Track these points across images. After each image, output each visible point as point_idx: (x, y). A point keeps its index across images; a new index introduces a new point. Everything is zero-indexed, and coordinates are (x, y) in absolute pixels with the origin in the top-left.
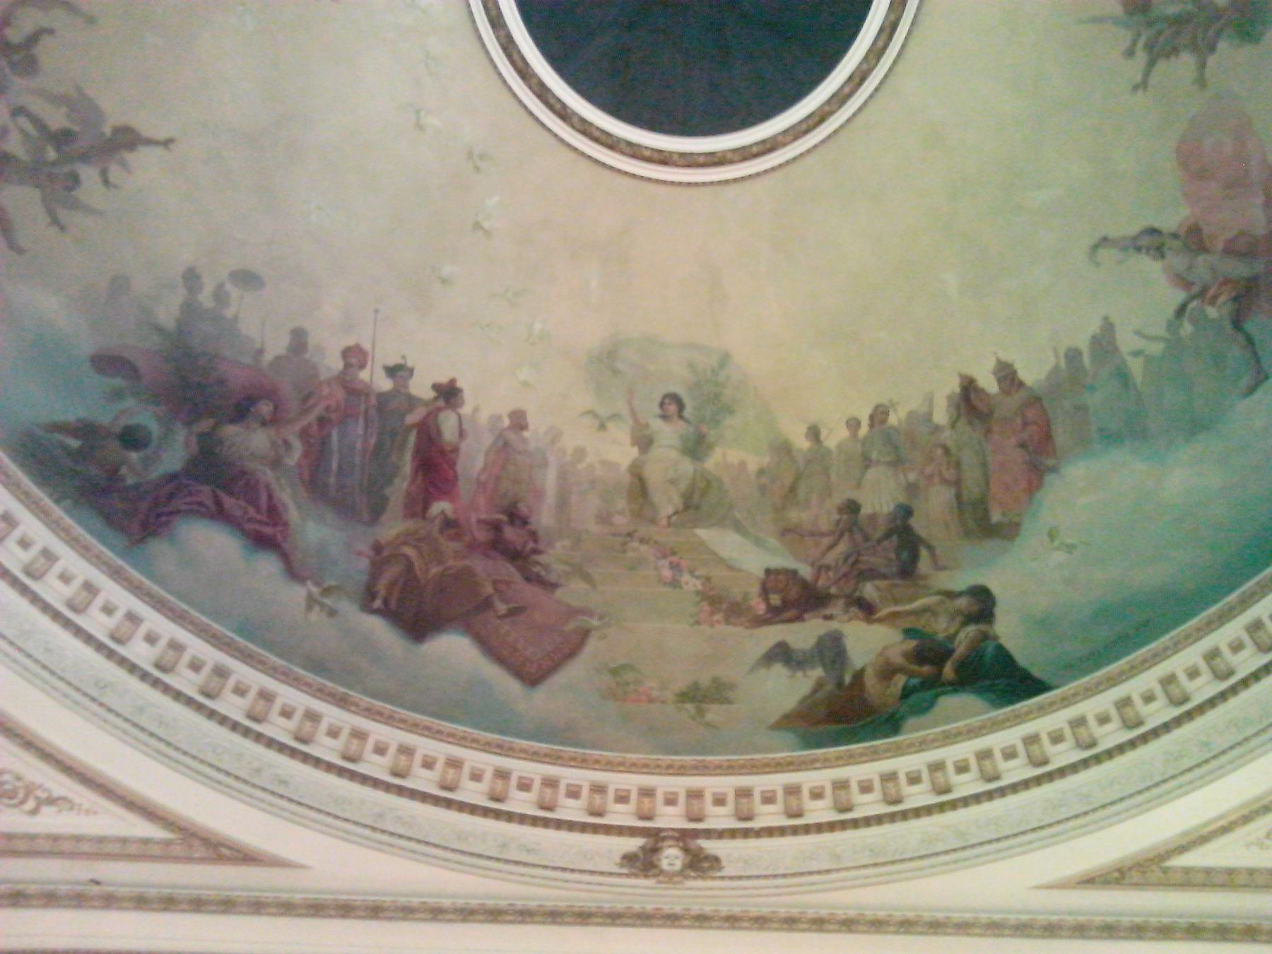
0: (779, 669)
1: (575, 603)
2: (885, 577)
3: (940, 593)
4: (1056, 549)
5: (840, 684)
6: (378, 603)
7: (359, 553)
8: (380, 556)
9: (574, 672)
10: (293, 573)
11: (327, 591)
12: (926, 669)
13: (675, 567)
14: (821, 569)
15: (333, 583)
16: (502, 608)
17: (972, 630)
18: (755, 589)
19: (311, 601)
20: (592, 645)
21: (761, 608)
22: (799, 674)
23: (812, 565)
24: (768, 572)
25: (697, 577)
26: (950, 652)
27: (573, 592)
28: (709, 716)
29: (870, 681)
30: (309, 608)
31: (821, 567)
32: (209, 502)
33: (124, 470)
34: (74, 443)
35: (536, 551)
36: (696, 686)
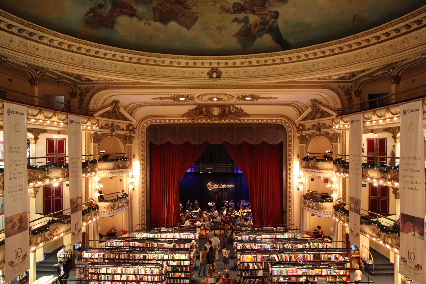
0: (235, 23)
1: (195, 11)
2: (258, 6)
3: (269, 11)
4: (294, 7)
5: (247, 27)
6: (157, 19)
7: (150, 10)
8: (154, 10)
9: (196, 25)
10: (140, 19)
11: (147, 20)
12: (263, 27)
13: (215, 2)
14: (245, 3)
15: (148, 18)
16: (180, 14)
17: (273, 19)
18: (232, 7)
19: (145, 23)
20: (199, 19)
21: (233, 11)
22: (239, 24)
23: (244, 2)
24: (234, 3)
25: (220, 4)
26: (268, 24)
27: (194, 9)
28: (222, 33)
29: (252, 26)
30: (145, 25)
31: (246, 3)
32: (119, 11)
33: (102, 14)
34: (92, 15)
35: (185, 2)
36: (219, 27)
